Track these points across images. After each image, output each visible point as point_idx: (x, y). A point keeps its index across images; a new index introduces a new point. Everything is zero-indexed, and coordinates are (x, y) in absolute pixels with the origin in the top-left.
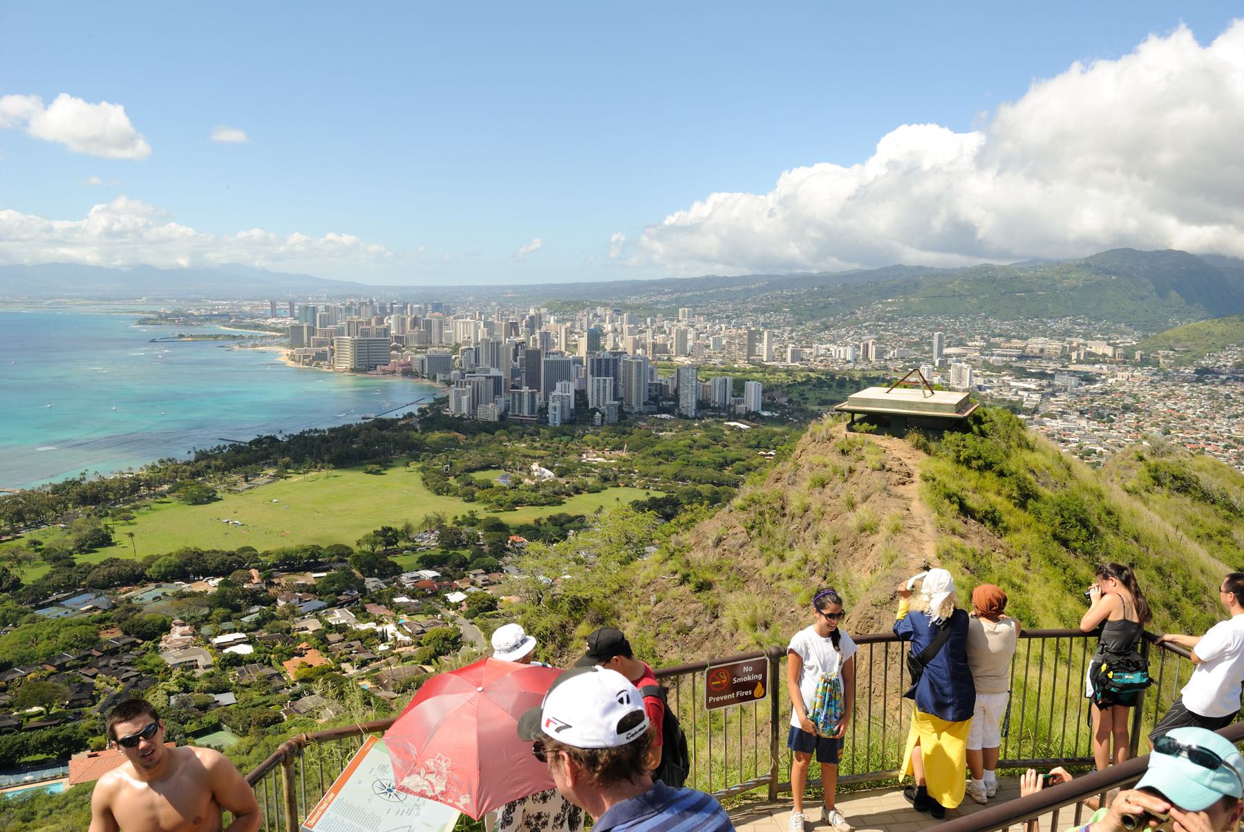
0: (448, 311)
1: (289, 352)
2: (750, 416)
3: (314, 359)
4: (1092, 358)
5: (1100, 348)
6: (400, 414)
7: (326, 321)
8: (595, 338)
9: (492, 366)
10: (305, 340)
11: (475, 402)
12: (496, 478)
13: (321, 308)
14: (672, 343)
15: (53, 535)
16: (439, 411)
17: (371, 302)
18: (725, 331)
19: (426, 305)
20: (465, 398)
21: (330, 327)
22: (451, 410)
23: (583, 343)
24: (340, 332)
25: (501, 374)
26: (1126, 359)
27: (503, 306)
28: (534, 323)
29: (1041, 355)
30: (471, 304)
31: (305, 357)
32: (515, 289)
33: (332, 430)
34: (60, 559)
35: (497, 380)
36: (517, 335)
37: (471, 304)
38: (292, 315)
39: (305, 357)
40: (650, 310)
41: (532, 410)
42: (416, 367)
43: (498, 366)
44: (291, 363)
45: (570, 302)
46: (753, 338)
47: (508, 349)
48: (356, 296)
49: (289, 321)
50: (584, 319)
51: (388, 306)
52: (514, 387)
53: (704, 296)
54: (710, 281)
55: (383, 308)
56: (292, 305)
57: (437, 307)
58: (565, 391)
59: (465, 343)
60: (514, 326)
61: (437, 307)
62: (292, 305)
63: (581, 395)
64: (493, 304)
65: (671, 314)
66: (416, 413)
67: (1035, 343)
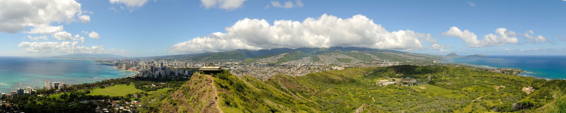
2: (186, 76)
4: (236, 65)
5: (237, 63)
8: (162, 64)
11: (143, 74)
12: (146, 86)
14: (174, 65)
15: (82, 91)
18: (182, 63)
22: (139, 76)
23: (160, 65)
26: (240, 64)
28: (152, 62)
29: (229, 65)
34: (83, 94)
40: (170, 60)
45: (158, 59)
46: (186, 64)
50: (160, 61)
53: (179, 58)
54: (179, 55)
58: (157, 72)
60: (149, 63)
63: (160, 73)
65: (174, 60)
67: (228, 63)
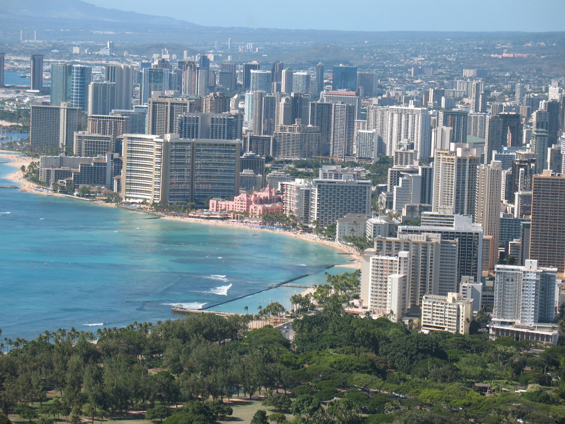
0: (368, 88)
1: (27, 162)
3: (79, 179)
6: (253, 305)
7: (107, 98)
9: (459, 210)
10: (62, 139)
13: (96, 71)
16: (336, 303)
17: (205, 61)
19: (321, 71)
20: (394, 279)
21: (114, 113)
24: (136, 125)
25: (478, 227)
27: (488, 80)
30: (419, 72)
31: (60, 175)
32: (517, 40)
33: (107, 334)
35: (468, 241)
36: (517, 143)
37: (419, 72)
38: (37, 82)
39: (60, 175)
41: (543, 317)
42: (291, 205)
43: (471, 211)
44: (29, 187)
47: (495, 174)
48: (175, 49)
49: (30, 97)
51: (240, 70)
52: (503, 259)
55: (228, 74)
56: (37, 61)
57: (344, 77)
59: (403, 157)
61: (344, 77)
62: (37, 61)
64: (468, 73)
66: (290, 307)
